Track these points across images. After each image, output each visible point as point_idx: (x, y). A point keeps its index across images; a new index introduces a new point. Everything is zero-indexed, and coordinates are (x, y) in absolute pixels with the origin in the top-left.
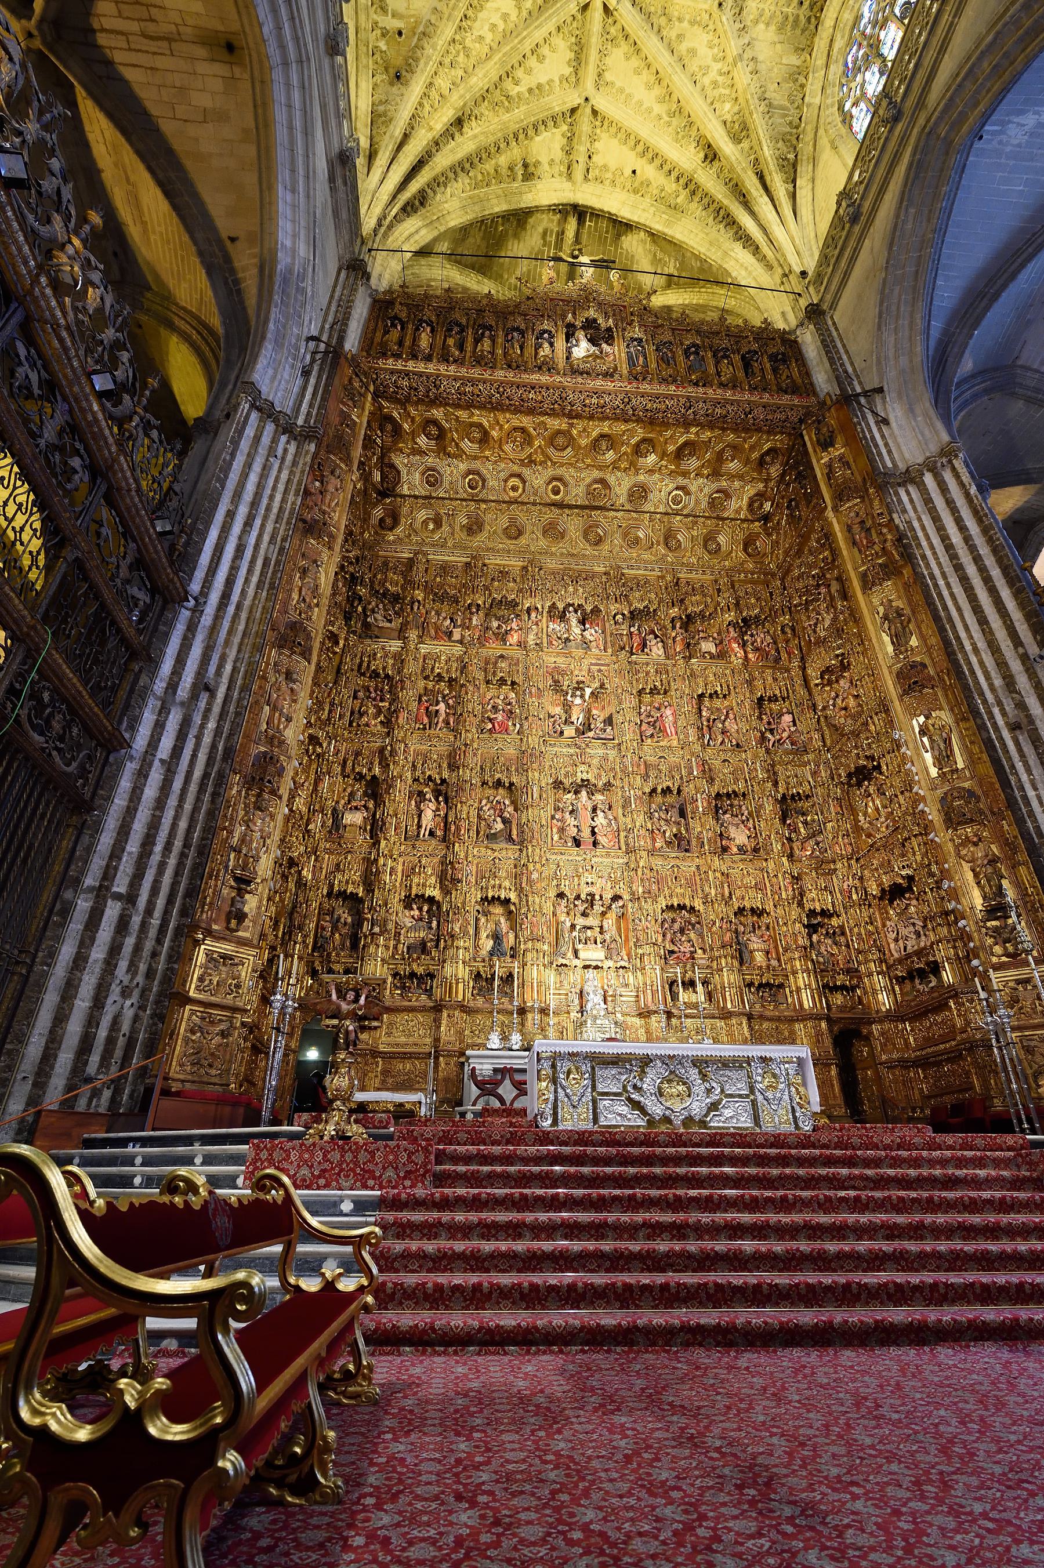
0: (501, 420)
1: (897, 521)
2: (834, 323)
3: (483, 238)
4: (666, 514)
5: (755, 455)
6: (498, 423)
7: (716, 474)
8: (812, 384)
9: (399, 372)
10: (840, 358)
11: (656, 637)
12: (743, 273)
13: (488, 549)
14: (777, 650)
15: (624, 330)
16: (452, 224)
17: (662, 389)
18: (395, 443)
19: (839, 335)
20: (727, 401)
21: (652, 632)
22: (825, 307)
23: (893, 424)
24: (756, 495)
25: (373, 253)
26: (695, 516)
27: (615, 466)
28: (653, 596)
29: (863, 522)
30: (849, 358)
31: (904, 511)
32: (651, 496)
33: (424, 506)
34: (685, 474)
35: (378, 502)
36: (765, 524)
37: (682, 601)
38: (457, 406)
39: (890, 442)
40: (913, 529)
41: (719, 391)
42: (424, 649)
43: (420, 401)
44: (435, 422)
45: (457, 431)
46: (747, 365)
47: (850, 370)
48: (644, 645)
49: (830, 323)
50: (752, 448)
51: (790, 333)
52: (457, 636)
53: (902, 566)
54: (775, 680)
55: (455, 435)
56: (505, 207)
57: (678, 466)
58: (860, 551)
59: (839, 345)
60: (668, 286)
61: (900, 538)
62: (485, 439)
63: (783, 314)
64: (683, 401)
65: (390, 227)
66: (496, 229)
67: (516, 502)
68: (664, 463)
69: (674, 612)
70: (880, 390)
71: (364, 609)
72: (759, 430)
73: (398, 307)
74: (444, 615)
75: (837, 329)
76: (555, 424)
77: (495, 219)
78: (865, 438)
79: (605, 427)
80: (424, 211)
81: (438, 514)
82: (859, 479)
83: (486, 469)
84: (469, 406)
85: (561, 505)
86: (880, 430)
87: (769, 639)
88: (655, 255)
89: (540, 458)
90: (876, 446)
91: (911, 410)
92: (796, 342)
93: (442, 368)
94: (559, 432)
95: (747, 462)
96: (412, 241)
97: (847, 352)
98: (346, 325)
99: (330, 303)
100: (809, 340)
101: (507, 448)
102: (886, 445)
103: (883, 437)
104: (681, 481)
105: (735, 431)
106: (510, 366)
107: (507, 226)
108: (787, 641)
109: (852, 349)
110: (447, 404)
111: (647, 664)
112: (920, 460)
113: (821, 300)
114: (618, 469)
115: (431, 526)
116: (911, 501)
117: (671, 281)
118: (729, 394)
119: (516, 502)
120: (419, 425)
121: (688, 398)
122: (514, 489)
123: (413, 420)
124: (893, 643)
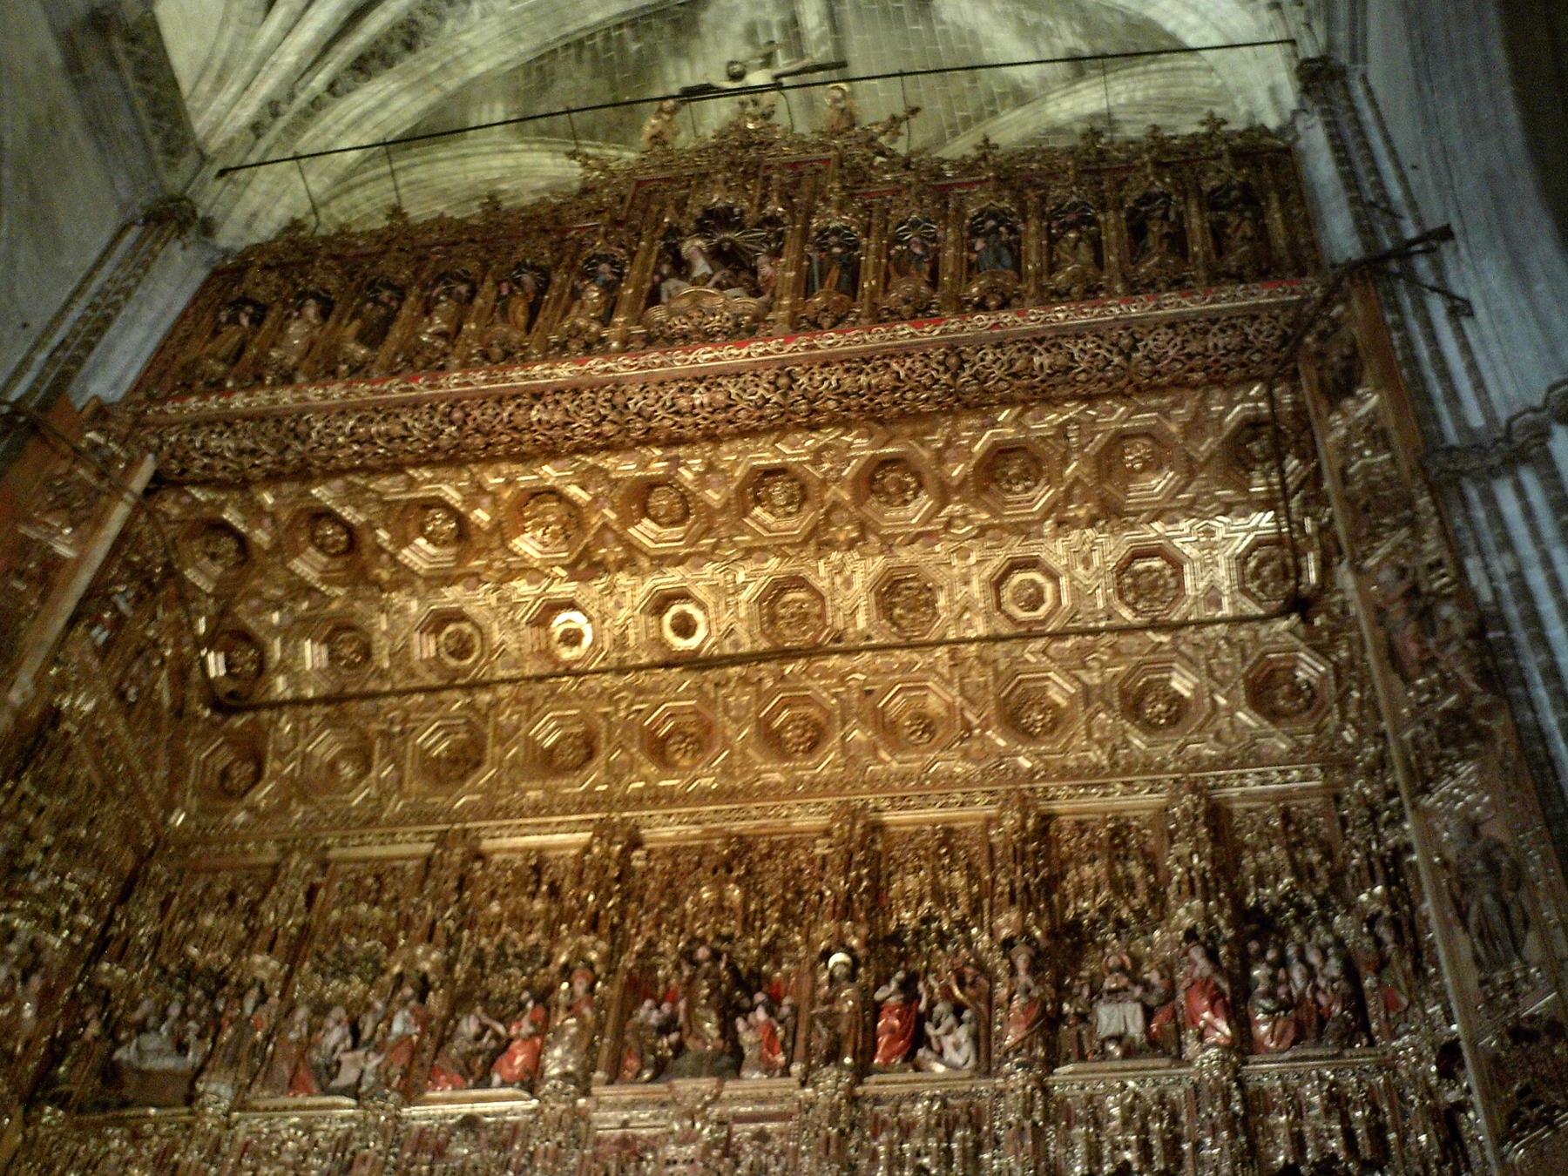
0: (492, 481)
1: (1476, 577)
2: (1369, 91)
3: (596, 74)
4: (995, 639)
5: (1206, 446)
6: (480, 489)
7: (1111, 513)
8: (1313, 245)
9: (210, 422)
10: (1375, 170)
11: (958, 1010)
12: (1191, 19)
13: (491, 815)
14: (1356, 1001)
15: (809, 215)
16: (479, 68)
17: (876, 337)
18: (241, 580)
19: (1379, 118)
20: (1062, 333)
21: (947, 993)
22: (1343, 58)
23: (1481, 313)
24: (1257, 544)
25: (242, 175)
26: (1083, 632)
27: (818, 540)
28: (958, 880)
29: (1413, 592)
30: (1398, 165)
31: (1507, 543)
32: (942, 601)
33: (328, 722)
34: (1023, 530)
35: (215, 726)
36: (1306, 619)
37: (1052, 884)
38: (372, 472)
39: (1480, 358)
40: (1524, 593)
41: (1034, 313)
42: (248, 1126)
43: (273, 478)
44: (328, 515)
45: (387, 528)
46: (1137, 231)
47: (1396, 192)
48: (915, 1039)
49: (1359, 91)
50: (1194, 427)
51: (1281, 132)
52: (347, 1076)
53: (1487, 711)
54: (1337, 1102)
55: (383, 535)
56: (616, 8)
57: (995, 514)
58: (1407, 680)
59: (1376, 140)
60: (1080, 75)
61: (1483, 622)
62: (463, 533)
63: (1273, 91)
64: (938, 355)
65: (316, 105)
66: (622, 50)
67: (569, 672)
68: (954, 508)
69: (1007, 923)
70: (1446, 233)
71: (111, 1031)
72: (1180, 384)
73: (254, 274)
74: (338, 1012)
75: (1373, 103)
76: (625, 467)
77: (610, 31)
78: (1413, 361)
79: (764, 455)
80: (410, 60)
81: (364, 737)
82: (1407, 476)
83: (477, 601)
84: (397, 468)
85: (694, 662)
86: (1459, 333)
87: (1334, 967)
88: (1021, 21)
89: (611, 552)
90: (1445, 375)
91: (1519, 271)
92: (1288, 151)
93: (313, 394)
94: (651, 485)
95: (1191, 469)
96: (367, 126)
97: (1393, 153)
98: (89, 347)
99: (67, 306)
100: (1315, 139)
101: (527, 545)
102: (1473, 368)
103: (1465, 348)
104: (1017, 548)
105: (1121, 395)
106: (486, 356)
107: (649, 38)
108: (1381, 965)
109: (1399, 144)
110: (340, 472)
111: (914, 1098)
112: (1538, 401)
113: (1330, 45)
114: (831, 545)
115: (347, 771)
116: (1528, 512)
117: (1079, 65)
118: (1061, 314)
119: (569, 672)
120: (293, 526)
121: (953, 348)
122: (572, 638)
123: (274, 516)
124: (1477, 960)
